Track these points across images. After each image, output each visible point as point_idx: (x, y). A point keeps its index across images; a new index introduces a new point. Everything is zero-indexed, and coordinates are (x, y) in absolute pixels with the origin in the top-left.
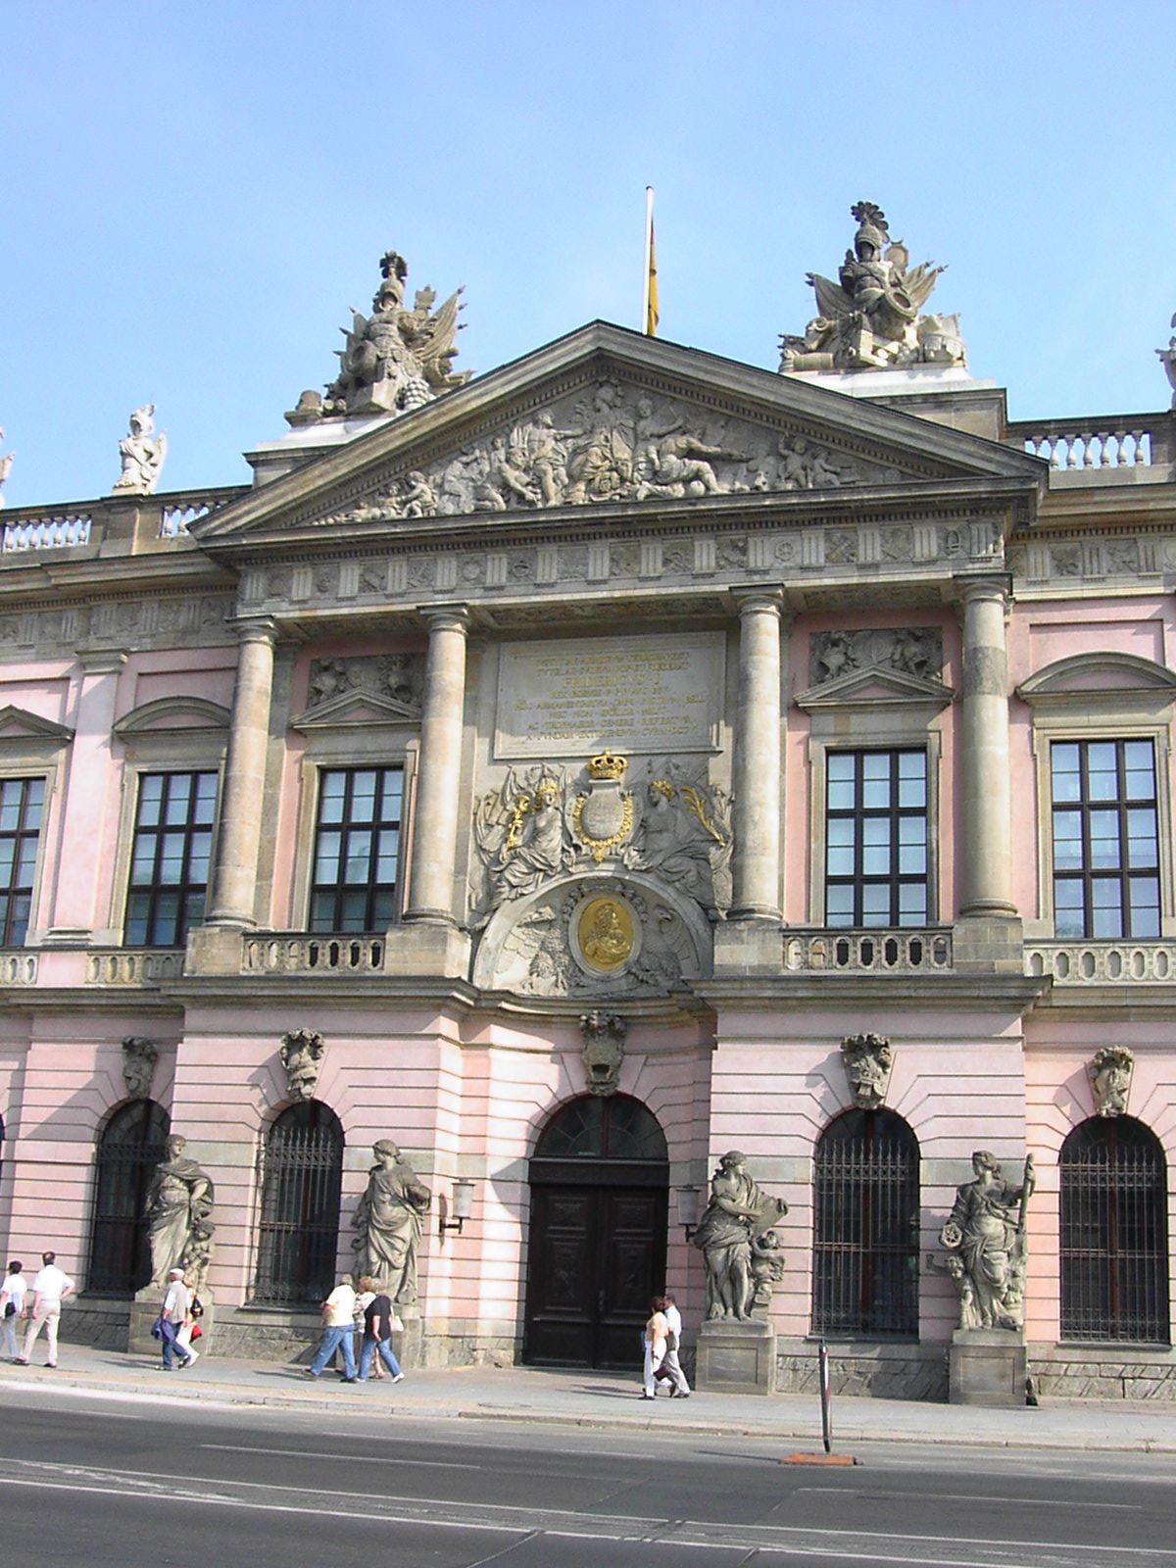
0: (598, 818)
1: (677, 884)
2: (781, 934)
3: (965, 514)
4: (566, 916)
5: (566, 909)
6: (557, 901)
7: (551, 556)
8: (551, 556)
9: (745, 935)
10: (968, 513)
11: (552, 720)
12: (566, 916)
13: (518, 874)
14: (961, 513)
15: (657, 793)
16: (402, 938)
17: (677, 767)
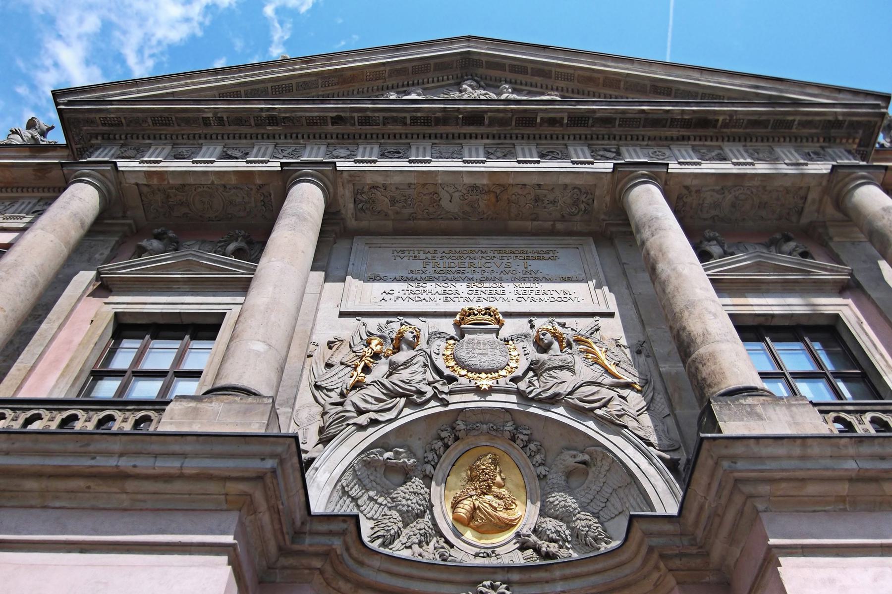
0: (477, 351)
1: (598, 412)
2: (816, 409)
3: (818, 141)
4: (429, 468)
5: (430, 456)
6: (418, 445)
7: (425, 148)
8: (425, 148)
9: (759, 409)
10: (821, 140)
11: (410, 288)
12: (429, 468)
13: (369, 399)
14: (816, 139)
15: (549, 335)
16: (195, 409)
17: (563, 325)
